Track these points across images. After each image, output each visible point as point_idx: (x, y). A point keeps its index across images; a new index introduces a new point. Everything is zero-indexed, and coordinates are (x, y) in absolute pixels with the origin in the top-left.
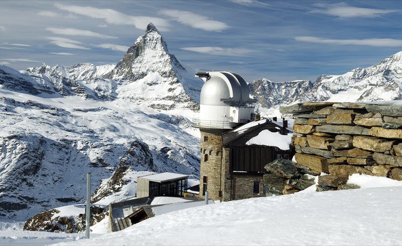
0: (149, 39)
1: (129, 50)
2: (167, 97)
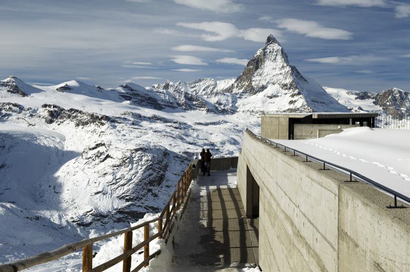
0: (269, 51)
1: (249, 63)
2: (288, 110)
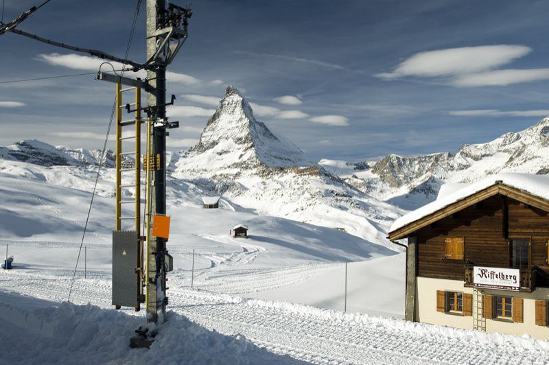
2: (233, 165)
